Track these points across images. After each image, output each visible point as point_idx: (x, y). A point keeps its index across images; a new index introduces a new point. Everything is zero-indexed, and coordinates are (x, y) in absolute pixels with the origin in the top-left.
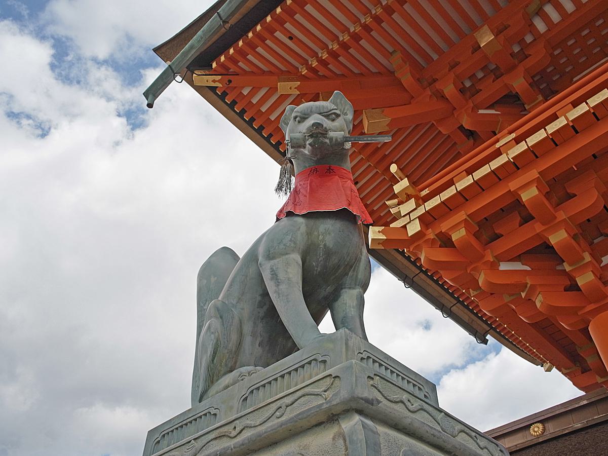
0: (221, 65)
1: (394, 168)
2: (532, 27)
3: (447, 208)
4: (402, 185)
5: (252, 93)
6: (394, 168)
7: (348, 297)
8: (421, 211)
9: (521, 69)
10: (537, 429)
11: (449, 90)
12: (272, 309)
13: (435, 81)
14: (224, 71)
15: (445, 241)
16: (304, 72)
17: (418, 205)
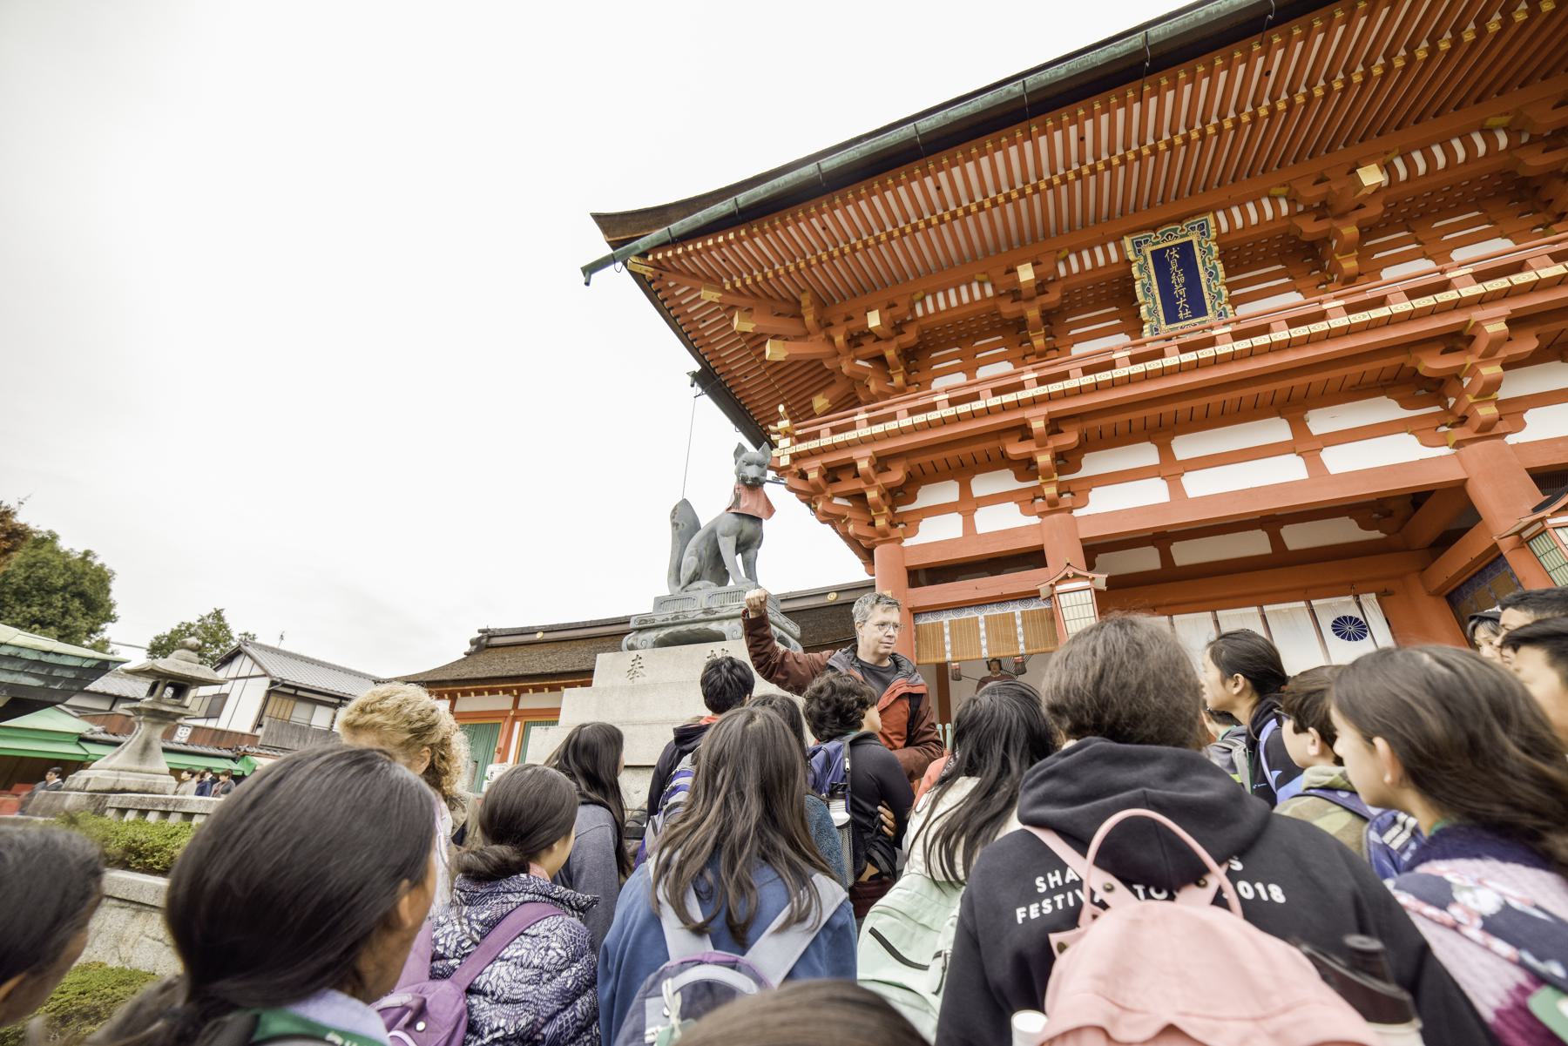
0: (655, 259)
1: (781, 408)
2: (913, 310)
3: (811, 454)
4: (784, 424)
5: (677, 286)
6: (781, 408)
7: (751, 553)
8: (793, 450)
9: (894, 343)
10: (832, 597)
11: (839, 339)
12: (719, 554)
13: (831, 324)
14: (658, 265)
15: (803, 475)
16: (728, 287)
17: (792, 444)
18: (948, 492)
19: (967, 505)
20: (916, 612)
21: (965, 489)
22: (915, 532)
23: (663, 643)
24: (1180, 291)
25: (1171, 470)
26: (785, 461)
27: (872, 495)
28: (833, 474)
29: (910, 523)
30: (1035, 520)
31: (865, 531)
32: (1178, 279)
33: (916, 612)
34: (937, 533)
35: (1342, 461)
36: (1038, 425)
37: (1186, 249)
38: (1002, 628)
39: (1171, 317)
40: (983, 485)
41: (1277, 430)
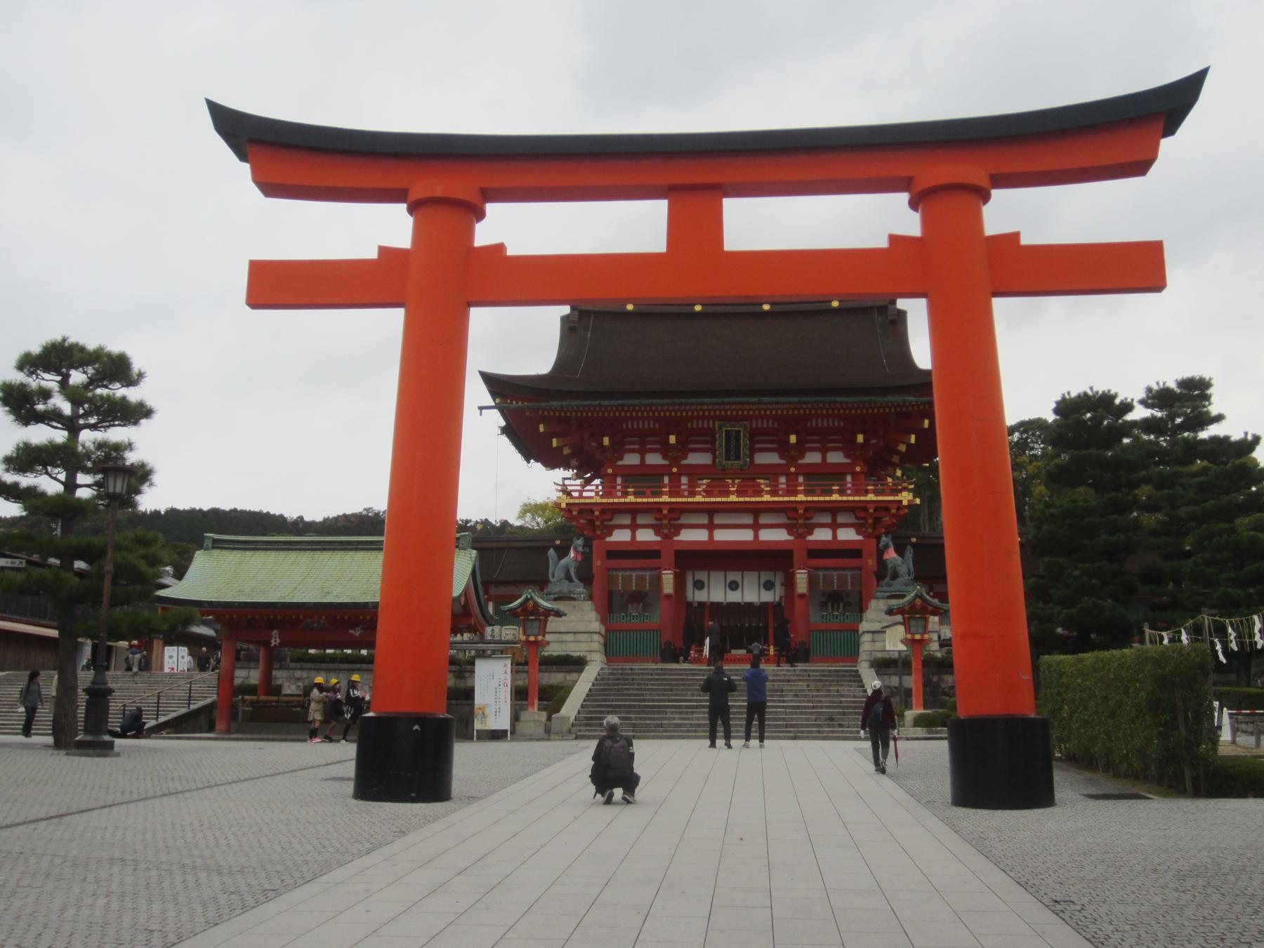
15: (570, 511)
18: (627, 520)
19: (634, 527)
20: (609, 569)
21: (634, 519)
22: (610, 535)
23: (555, 599)
24: (733, 447)
25: (711, 527)
26: (563, 506)
27: (598, 523)
28: (581, 512)
29: (610, 530)
30: (658, 539)
31: (590, 535)
32: (733, 443)
33: (609, 569)
34: (621, 536)
35: (767, 535)
36: (665, 512)
37: (738, 432)
38: (641, 579)
39: (727, 458)
40: (640, 520)
41: (749, 520)
